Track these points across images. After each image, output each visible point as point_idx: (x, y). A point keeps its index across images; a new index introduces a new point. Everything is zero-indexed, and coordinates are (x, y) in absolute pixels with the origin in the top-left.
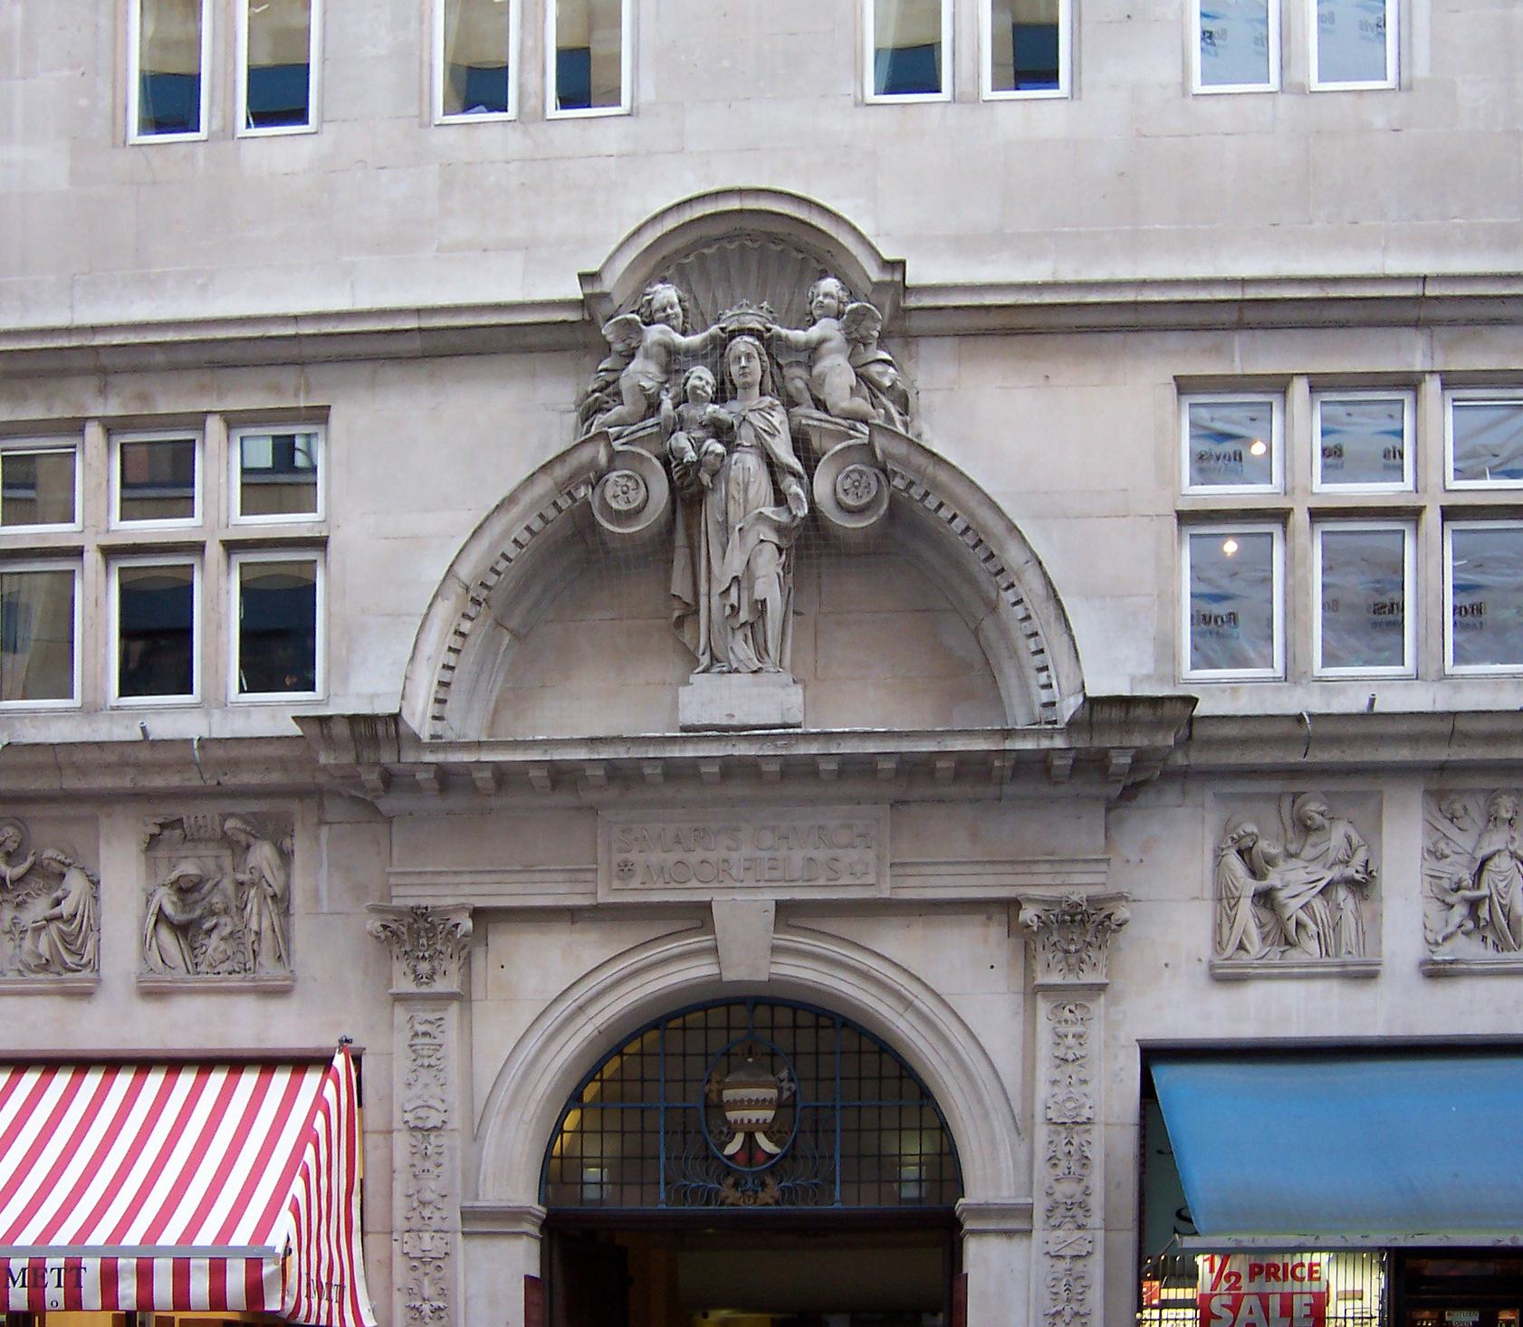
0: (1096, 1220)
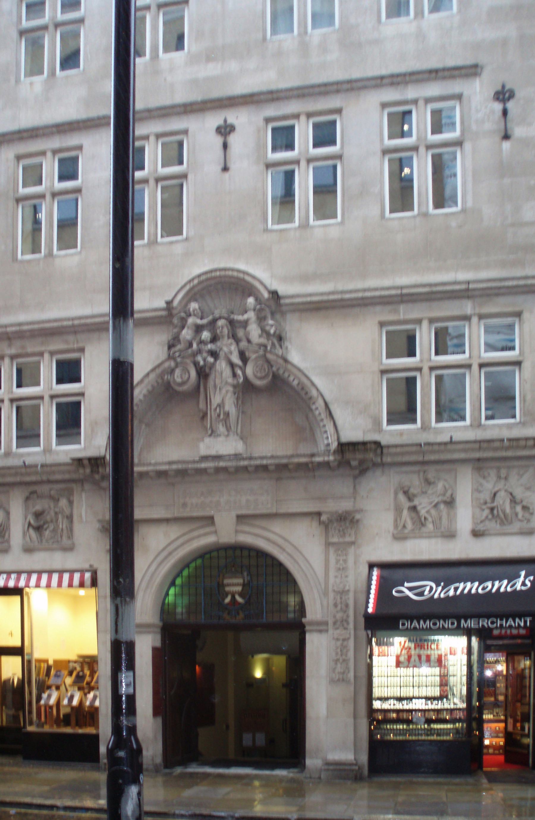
0: (351, 626)
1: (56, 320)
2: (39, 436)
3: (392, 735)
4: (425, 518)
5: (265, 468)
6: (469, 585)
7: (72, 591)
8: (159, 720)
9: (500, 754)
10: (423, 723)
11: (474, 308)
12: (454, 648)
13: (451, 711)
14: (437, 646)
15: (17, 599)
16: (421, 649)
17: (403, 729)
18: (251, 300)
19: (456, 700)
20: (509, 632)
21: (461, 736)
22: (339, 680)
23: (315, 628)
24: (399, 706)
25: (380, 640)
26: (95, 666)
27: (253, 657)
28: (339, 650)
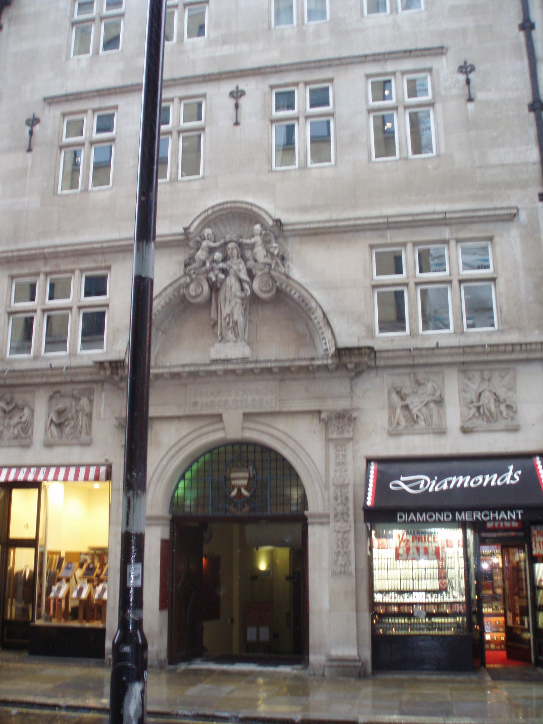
1: (87, 243)
2: (66, 341)
3: (394, 629)
4: (417, 416)
5: (269, 370)
6: (461, 479)
7: (87, 484)
8: (165, 613)
9: (501, 650)
10: (424, 617)
11: (452, 234)
12: (450, 540)
13: (451, 604)
14: (434, 538)
15: (35, 491)
16: (419, 541)
17: (405, 623)
18: (257, 227)
19: (456, 593)
20: (502, 524)
21: (462, 630)
22: (340, 572)
23: (317, 520)
24: (400, 599)
25: (379, 533)
26: (105, 558)
27: (257, 549)
28: (340, 542)
